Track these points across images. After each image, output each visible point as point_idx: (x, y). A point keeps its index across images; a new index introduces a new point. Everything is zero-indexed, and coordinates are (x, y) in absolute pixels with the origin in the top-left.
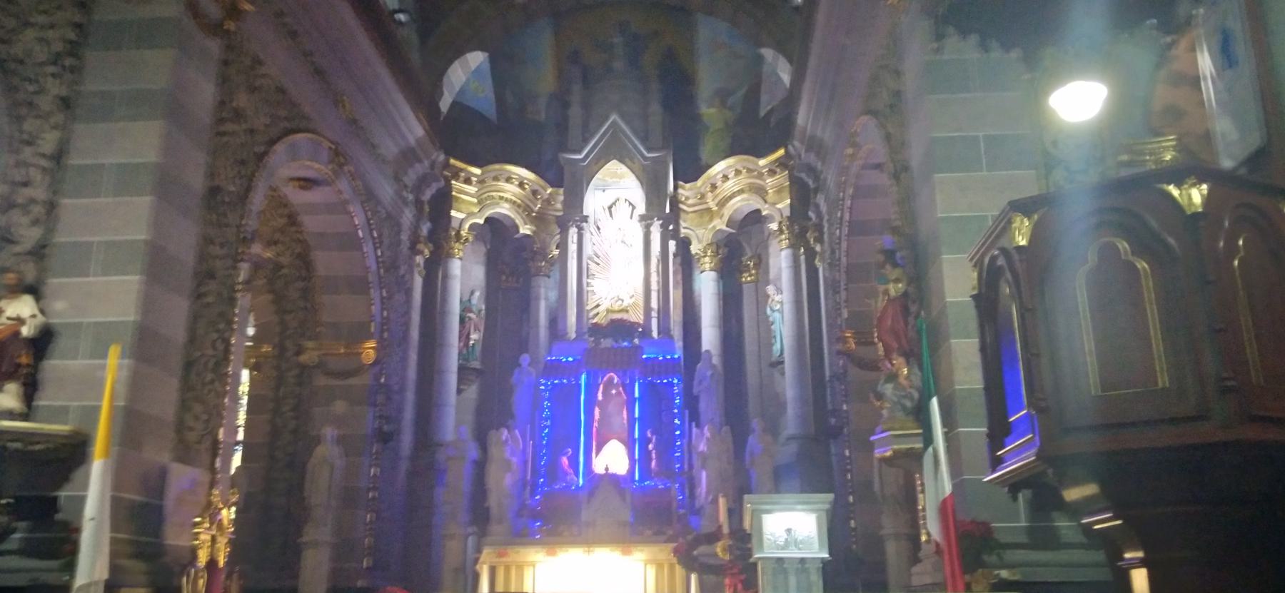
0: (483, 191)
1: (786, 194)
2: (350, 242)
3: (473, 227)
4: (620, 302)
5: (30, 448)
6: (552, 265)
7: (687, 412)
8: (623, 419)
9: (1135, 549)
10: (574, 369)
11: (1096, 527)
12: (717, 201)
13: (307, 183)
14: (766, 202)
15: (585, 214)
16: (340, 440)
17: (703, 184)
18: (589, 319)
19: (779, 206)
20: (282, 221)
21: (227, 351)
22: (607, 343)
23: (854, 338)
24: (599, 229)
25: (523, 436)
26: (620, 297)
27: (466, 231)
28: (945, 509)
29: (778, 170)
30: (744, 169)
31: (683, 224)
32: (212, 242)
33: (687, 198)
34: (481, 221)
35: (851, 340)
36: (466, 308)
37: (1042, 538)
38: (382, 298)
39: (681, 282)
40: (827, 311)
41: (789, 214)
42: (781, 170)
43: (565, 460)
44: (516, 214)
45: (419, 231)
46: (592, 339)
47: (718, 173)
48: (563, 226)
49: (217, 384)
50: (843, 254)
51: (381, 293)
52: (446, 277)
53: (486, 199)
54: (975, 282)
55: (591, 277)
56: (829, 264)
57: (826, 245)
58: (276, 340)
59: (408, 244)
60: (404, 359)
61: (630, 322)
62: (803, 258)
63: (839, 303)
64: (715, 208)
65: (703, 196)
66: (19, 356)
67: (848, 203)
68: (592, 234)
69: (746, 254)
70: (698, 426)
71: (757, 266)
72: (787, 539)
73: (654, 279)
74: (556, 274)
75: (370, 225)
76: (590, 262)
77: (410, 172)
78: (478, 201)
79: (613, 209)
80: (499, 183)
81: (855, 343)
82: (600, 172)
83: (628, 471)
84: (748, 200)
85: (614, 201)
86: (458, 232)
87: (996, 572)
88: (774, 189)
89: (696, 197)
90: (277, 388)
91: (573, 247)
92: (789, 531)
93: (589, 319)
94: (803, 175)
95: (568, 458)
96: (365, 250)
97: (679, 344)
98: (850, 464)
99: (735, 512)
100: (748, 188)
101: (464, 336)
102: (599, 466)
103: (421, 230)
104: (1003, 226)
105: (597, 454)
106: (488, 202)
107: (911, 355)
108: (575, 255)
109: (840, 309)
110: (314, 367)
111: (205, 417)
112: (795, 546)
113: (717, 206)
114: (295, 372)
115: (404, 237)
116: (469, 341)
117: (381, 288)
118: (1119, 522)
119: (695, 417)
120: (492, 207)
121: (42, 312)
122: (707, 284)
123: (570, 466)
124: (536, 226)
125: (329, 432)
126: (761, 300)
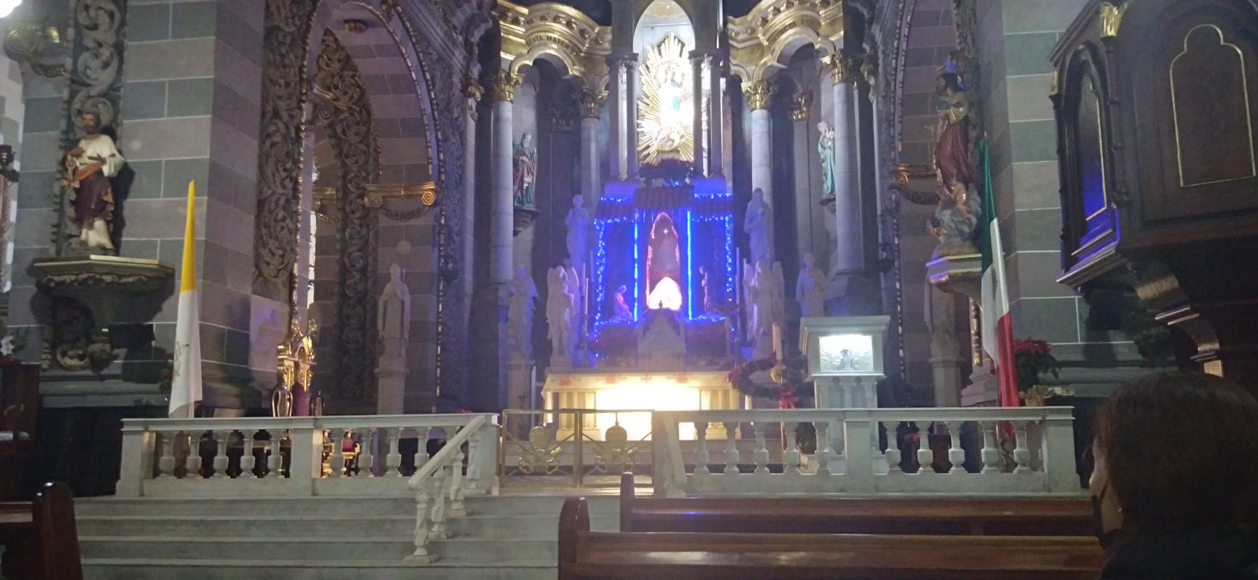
0: (529, 32)
1: (840, 25)
2: (404, 85)
3: (523, 69)
4: (670, 142)
5: (124, 280)
6: (601, 106)
7: (738, 249)
8: (675, 257)
9: (1209, 341)
10: (628, 209)
11: (1169, 323)
12: (768, 35)
13: (359, 25)
14: (818, 35)
15: (635, 51)
16: (406, 278)
17: (753, 19)
18: (639, 160)
19: (833, 39)
20: (336, 66)
21: (295, 190)
22: (659, 182)
23: (908, 172)
25: (580, 275)
26: (672, 137)
27: (516, 73)
28: (1002, 327)
31: (733, 61)
32: (274, 83)
33: (737, 34)
34: (530, 63)
35: (905, 174)
36: (519, 151)
37: (1097, 356)
38: (438, 140)
39: (730, 122)
40: (880, 147)
41: (842, 47)
43: (620, 298)
44: (565, 55)
45: (470, 73)
46: (644, 179)
47: (769, 7)
48: (612, 62)
49: (288, 221)
50: (899, 85)
51: (437, 136)
52: (498, 120)
53: (535, 41)
54: (1055, 82)
55: (640, 118)
56: (884, 97)
57: (881, 78)
58: (340, 183)
59: (459, 86)
60: (462, 200)
61: (681, 161)
62: (856, 92)
63: (893, 137)
64: (766, 43)
65: (754, 31)
66: (106, 194)
67: (905, 31)
68: (641, 74)
69: (797, 91)
70: (749, 262)
71: (808, 103)
72: (843, 360)
73: (704, 117)
74: (606, 116)
75: (422, 67)
76: (639, 102)
77: (458, 12)
79: (662, 48)
80: (548, 23)
81: (908, 177)
83: (681, 306)
84: (801, 34)
86: (508, 74)
87: (1050, 389)
88: (828, 21)
89: (747, 32)
90: (343, 230)
91: (623, 87)
92: (845, 352)
93: (639, 160)
95: (623, 295)
97: (730, 184)
98: (900, 296)
99: (791, 334)
101: (518, 180)
102: (653, 301)
103: (472, 72)
104: (1089, 18)
105: (651, 290)
106: (536, 43)
107: (973, 181)
108: (625, 96)
109: (894, 143)
110: (379, 209)
111: (281, 252)
112: (851, 366)
114: (358, 214)
115: (456, 79)
116: (523, 186)
117: (437, 131)
118: (1197, 315)
119: (747, 254)
121: (120, 152)
122: (757, 123)
123: (626, 301)
124: (585, 66)
125: (395, 271)
126: (813, 137)
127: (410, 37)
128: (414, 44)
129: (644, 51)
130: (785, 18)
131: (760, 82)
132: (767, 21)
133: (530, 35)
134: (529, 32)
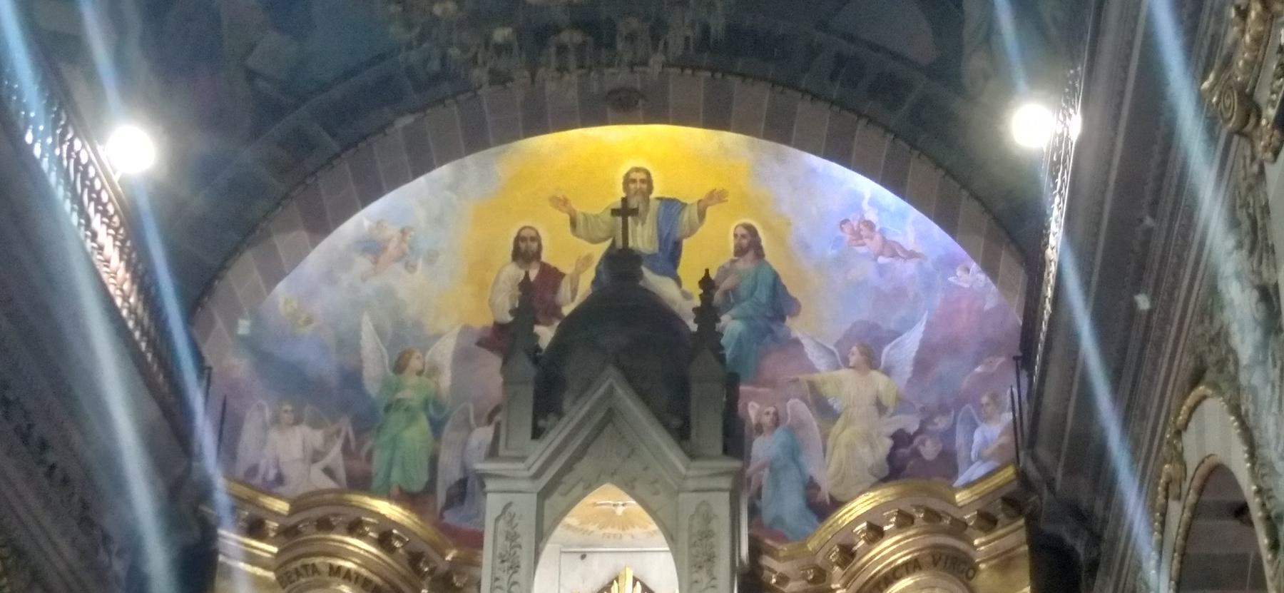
0: (287, 556)
29: (1001, 516)
30: (918, 511)
33: (783, 579)
42: (1008, 516)
78: (278, 578)
85: (607, 582)
88: (993, 562)
89: (804, 577)
94: (1065, 532)
100: (930, 559)
106: (303, 580)
132: (853, 555)
133: (286, 563)
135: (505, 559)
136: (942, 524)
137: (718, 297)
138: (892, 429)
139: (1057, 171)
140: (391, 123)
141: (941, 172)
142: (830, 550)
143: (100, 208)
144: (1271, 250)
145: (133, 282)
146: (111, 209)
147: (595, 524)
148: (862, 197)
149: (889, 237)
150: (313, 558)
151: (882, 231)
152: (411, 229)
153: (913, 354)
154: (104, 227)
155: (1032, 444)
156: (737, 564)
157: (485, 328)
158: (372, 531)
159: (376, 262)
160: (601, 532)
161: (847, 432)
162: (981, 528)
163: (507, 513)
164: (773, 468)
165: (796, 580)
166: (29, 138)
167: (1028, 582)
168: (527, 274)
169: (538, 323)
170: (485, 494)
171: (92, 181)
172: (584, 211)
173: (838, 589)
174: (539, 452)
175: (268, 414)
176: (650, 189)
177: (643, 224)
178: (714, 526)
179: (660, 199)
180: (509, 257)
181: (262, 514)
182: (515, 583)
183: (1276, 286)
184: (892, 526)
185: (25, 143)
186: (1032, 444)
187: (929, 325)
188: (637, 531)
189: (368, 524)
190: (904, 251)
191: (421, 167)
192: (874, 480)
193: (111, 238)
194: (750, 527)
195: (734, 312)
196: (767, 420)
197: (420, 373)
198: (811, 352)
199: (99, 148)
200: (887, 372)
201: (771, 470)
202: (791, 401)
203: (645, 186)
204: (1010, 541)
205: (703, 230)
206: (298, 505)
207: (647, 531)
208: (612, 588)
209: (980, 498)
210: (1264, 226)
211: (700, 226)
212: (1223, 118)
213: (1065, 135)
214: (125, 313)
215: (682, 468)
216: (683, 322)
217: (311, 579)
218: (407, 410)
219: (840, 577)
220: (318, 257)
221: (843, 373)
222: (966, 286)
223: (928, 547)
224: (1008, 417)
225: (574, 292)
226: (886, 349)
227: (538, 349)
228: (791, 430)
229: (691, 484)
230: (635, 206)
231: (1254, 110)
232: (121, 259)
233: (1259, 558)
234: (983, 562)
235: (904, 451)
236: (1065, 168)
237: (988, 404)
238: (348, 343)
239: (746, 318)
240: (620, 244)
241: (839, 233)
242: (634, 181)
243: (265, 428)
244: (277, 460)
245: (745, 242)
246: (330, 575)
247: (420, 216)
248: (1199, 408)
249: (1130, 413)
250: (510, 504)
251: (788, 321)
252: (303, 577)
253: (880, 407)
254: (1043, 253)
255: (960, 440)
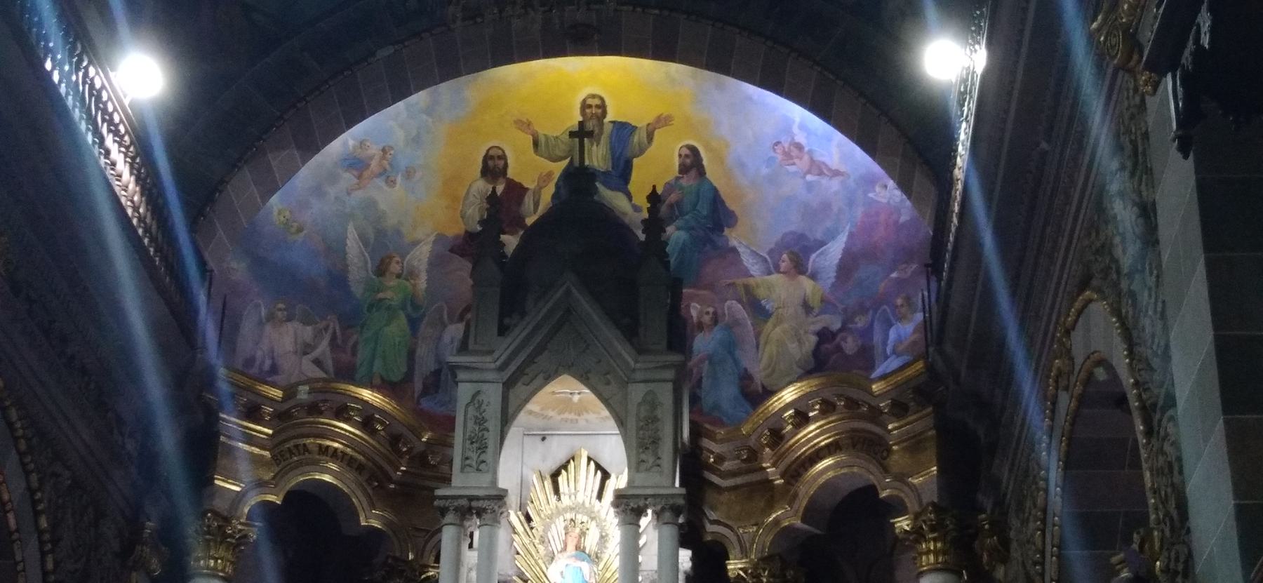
0: (283, 436)
1: (931, 453)
12: (782, 466)
14: (886, 470)
15: (502, 484)
19: (916, 481)
24: (528, 519)
30: (840, 400)
44: (353, 486)
65: (754, 455)
68: (514, 528)
75: (35, 503)
78: (273, 456)
79: (560, 479)
82: (535, 399)
89: (738, 457)
96: (18, 558)
106: (295, 458)
113: (782, 477)
120: (307, 468)
127: (16, 439)
128: (19, 453)
129: (523, 484)
130: (813, 433)
131: (766, 560)
134: (283, 436)
135: (474, 440)
136: (860, 411)
137: (664, 209)
138: (818, 327)
139: (965, 99)
140: (373, 54)
141: (863, 100)
142: (761, 434)
143: (112, 128)
144: (1149, 171)
145: (142, 195)
146: (122, 129)
147: (553, 410)
148: (794, 122)
149: (818, 158)
150: (305, 439)
151: (810, 152)
152: (392, 148)
153: (836, 261)
154: (116, 145)
155: (940, 341)
156: (680, 446)
157: (457, 237)
158: (356, 416)
159: (359, 177)
160: (559, 418)
161: (778, 329)
162: (894, 415)
163: (476, 402)
164: (710, 358)
165: (730, 460)
166: (48, 65)
167: (935, 462)
168: (494, 189)
169: (504, 233)
170: (456, 383)
171: (105, 104)
172: (546, 133)
173: (769, 467)
174: (503, 348)
175: (264, 312)
176: (604, 113)
177: (597, 146)
178: (659, 413)
179: (613, 122)
180: (479, 174)
181: (259, 400)
182: (483, 462)
183: (1154, 203)
184: (815, 413)
185: (45, 69)
186: (940, 341)
187: (851, 235)
188: (591, 417)
189: (353, 409)
190: (830, 170)
191: (401, 92)
192: (800, 371)
193: (122, 155)
194: (691, 412)
195: (679, 222)
196: (707, 319)
197: (399, 276)
198: (747, 260)
199: (111, 74)
200: (813, 277)
201: (710, 363)
202: (728, 303)
203: (600, 111)
204: (919, 426)
205: (652, 151)
206: (290, 392)
207: (600, 417)
208: (569, 466)
209: (896, 388)
210: (1144, 150)
211: (648, 147)
212: (1109, 54)
213: (971, 68)
214: (135, 221)
215: (632, 363)
216: (634, 234)
217: (302, 457)
218: (389, 308)
219: (770, 457)
220: (307, 174)
221: (775, 278)
222: (884, 201)
223: (847, 432)
224: (919, 316)
225: (536, 205)
226: (813, 256)
227: (504, 255)
228: (729, 327)
229: (639, 376)
230: (591, 129)
231: (1136, 49)
232: (131, 174)
233: (1136, 441)
234: (894, 445)
235: (828, 346)
236: (971, 97)
237: (902, 305)
238: (336, 249)
239: (689, 229)
240: (577, 163)
241: (772, 154)
242: (590, 106)
243: (261, 324)
244: (272, 351)
245: (688, 161)
246: (319, 454)
247: (399, 138)
248: (1086, 310)
249: (1026, 318)
250: (478, 393)
251: (727, 232)
252: (296, 456)
253: (807, 307)
254: (952, 173)
255: (877, 337)
